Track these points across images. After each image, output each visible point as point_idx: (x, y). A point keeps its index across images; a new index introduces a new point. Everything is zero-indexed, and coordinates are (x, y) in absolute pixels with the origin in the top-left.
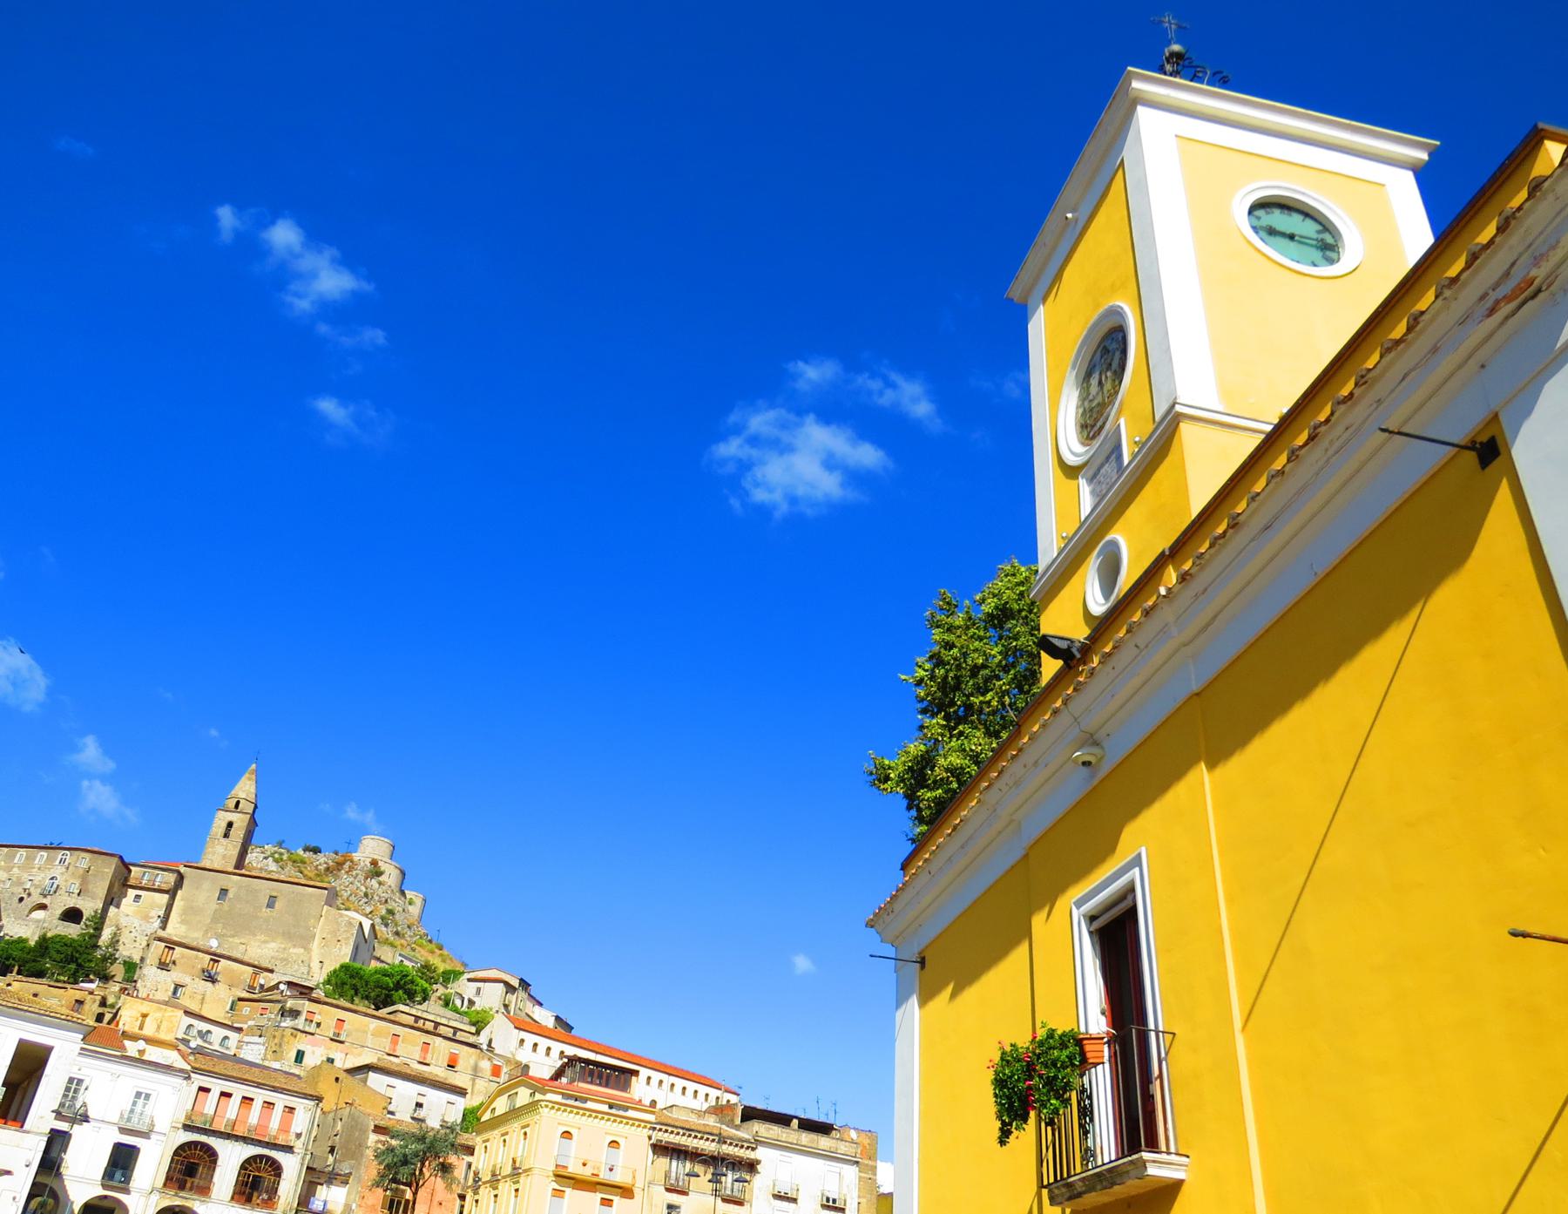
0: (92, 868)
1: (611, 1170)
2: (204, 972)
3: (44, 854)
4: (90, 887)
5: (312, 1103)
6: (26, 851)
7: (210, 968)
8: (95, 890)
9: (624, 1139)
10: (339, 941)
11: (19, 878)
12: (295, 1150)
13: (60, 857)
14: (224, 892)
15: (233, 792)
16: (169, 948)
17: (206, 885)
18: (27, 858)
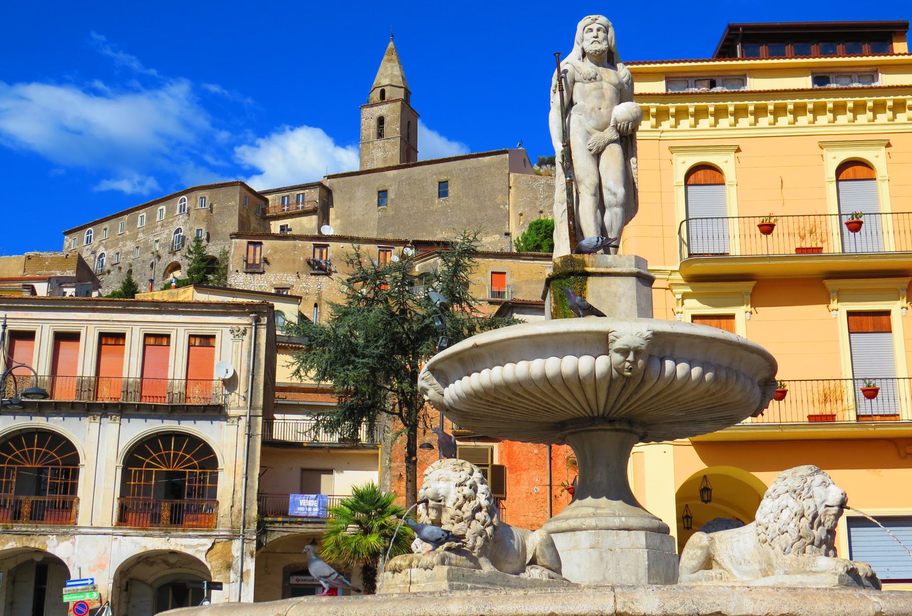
0: (215, 205)
1: (855, 226)
2: (309, 263)
3: (163, 207)
4: (219, 228)
5: (246, 320)
6: (146, 211)
7: (317, 257)
8: (224, 230)
9: (883, 151)
10: (541, 212)
11: (146, 243)
12: (231, 413)
13: (178, 205)
14: (383, 195)
15: (375, 83)
16: (255, 244)
17: (360, 193)
18: (148, 219)
